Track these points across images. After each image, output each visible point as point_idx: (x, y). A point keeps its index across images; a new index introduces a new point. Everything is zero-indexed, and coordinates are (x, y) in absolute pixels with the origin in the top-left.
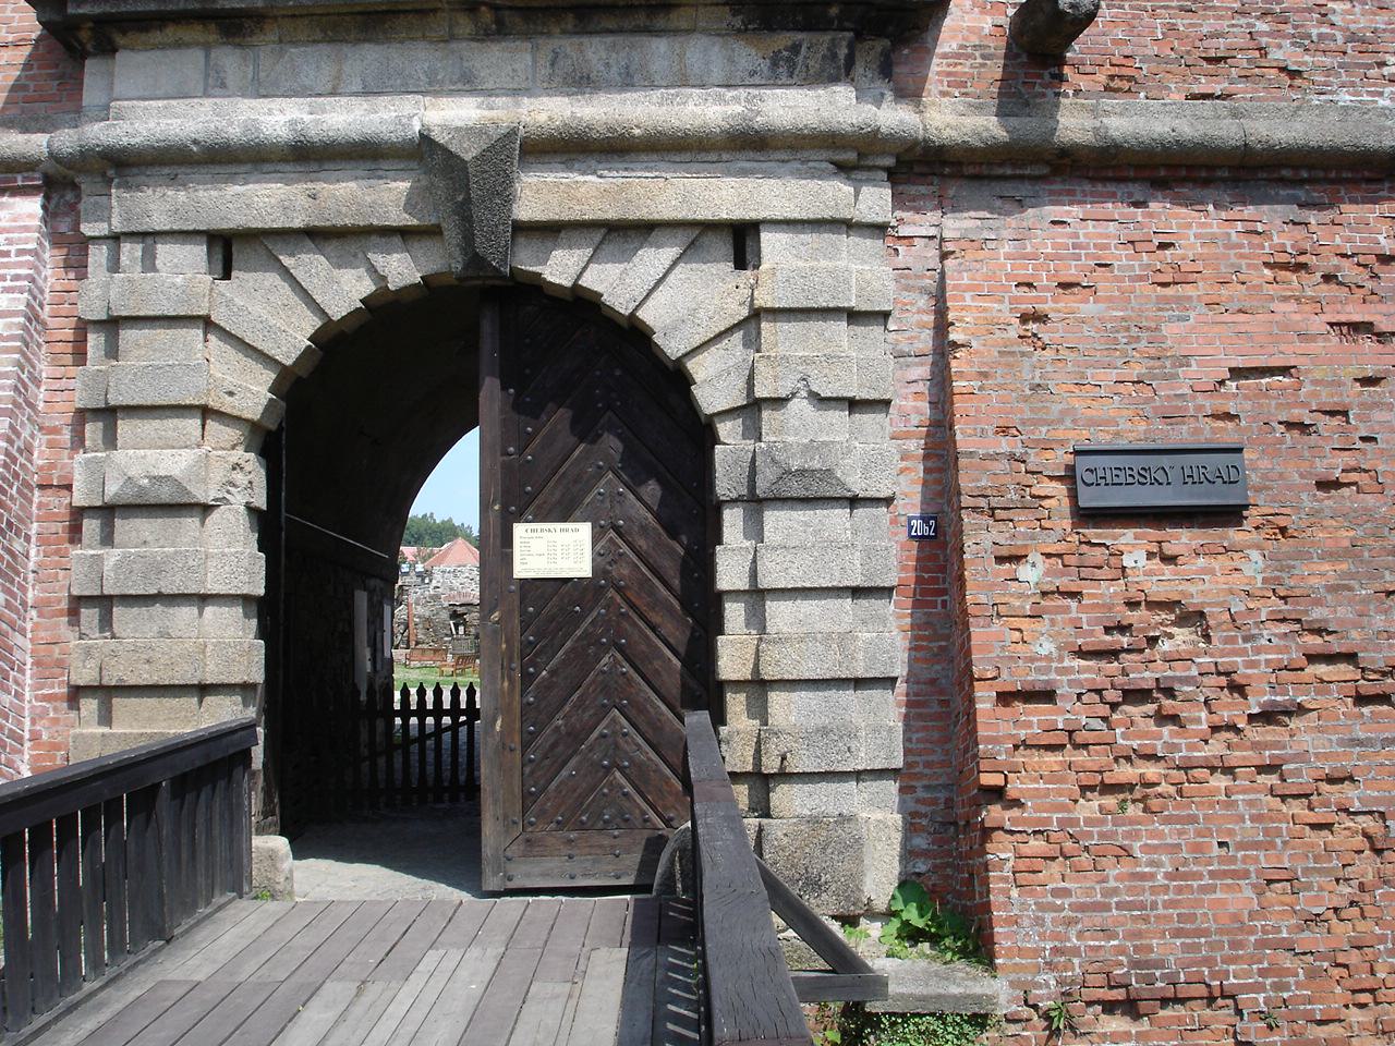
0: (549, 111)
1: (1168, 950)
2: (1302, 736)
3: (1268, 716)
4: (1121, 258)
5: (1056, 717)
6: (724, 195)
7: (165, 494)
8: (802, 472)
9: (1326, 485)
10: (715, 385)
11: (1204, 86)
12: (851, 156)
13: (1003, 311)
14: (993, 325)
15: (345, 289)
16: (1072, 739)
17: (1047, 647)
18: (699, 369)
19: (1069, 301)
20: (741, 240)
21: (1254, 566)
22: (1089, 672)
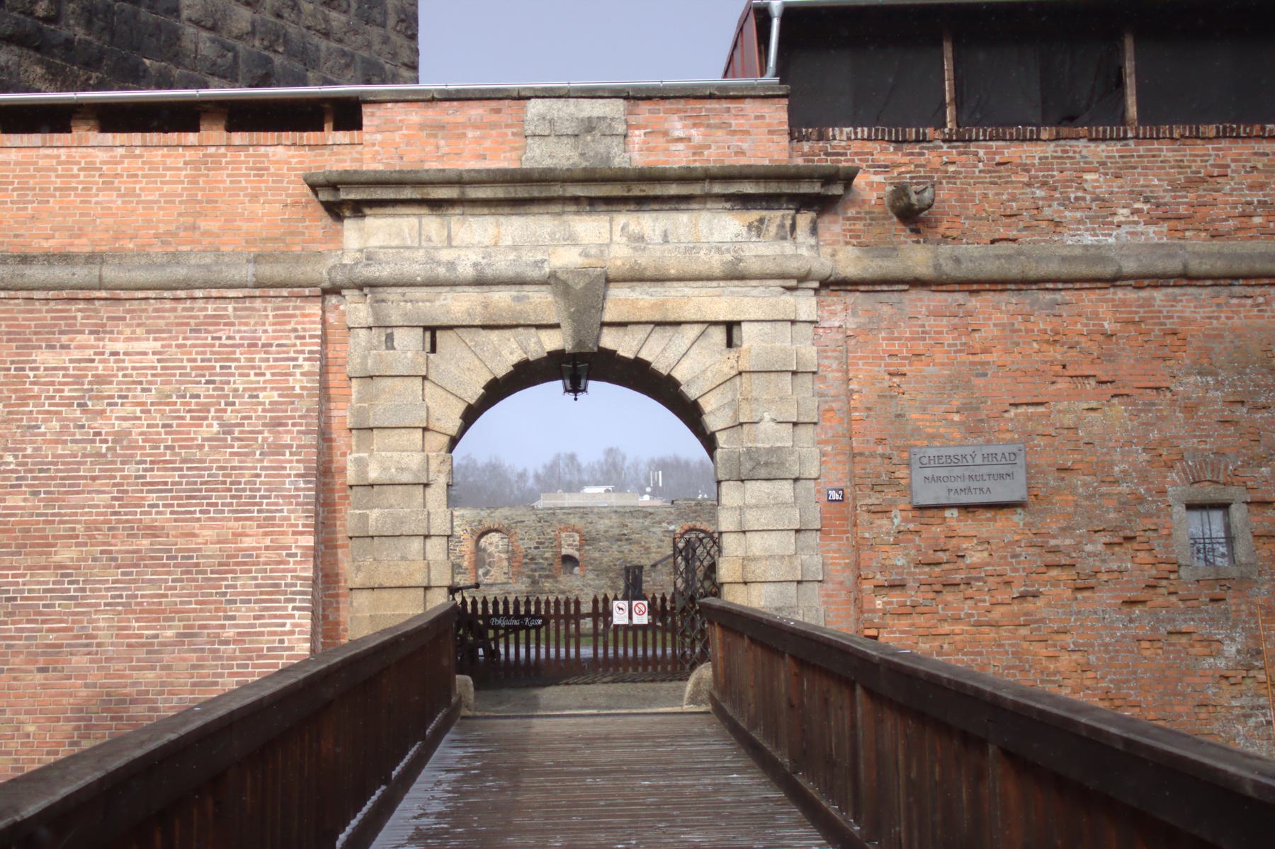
0: (620, 255)
3: (1023, 596)
4: (948, 339)
8: (766, 464)
11: (1002, 232)
12: (793, 283)
13: (880, 371)
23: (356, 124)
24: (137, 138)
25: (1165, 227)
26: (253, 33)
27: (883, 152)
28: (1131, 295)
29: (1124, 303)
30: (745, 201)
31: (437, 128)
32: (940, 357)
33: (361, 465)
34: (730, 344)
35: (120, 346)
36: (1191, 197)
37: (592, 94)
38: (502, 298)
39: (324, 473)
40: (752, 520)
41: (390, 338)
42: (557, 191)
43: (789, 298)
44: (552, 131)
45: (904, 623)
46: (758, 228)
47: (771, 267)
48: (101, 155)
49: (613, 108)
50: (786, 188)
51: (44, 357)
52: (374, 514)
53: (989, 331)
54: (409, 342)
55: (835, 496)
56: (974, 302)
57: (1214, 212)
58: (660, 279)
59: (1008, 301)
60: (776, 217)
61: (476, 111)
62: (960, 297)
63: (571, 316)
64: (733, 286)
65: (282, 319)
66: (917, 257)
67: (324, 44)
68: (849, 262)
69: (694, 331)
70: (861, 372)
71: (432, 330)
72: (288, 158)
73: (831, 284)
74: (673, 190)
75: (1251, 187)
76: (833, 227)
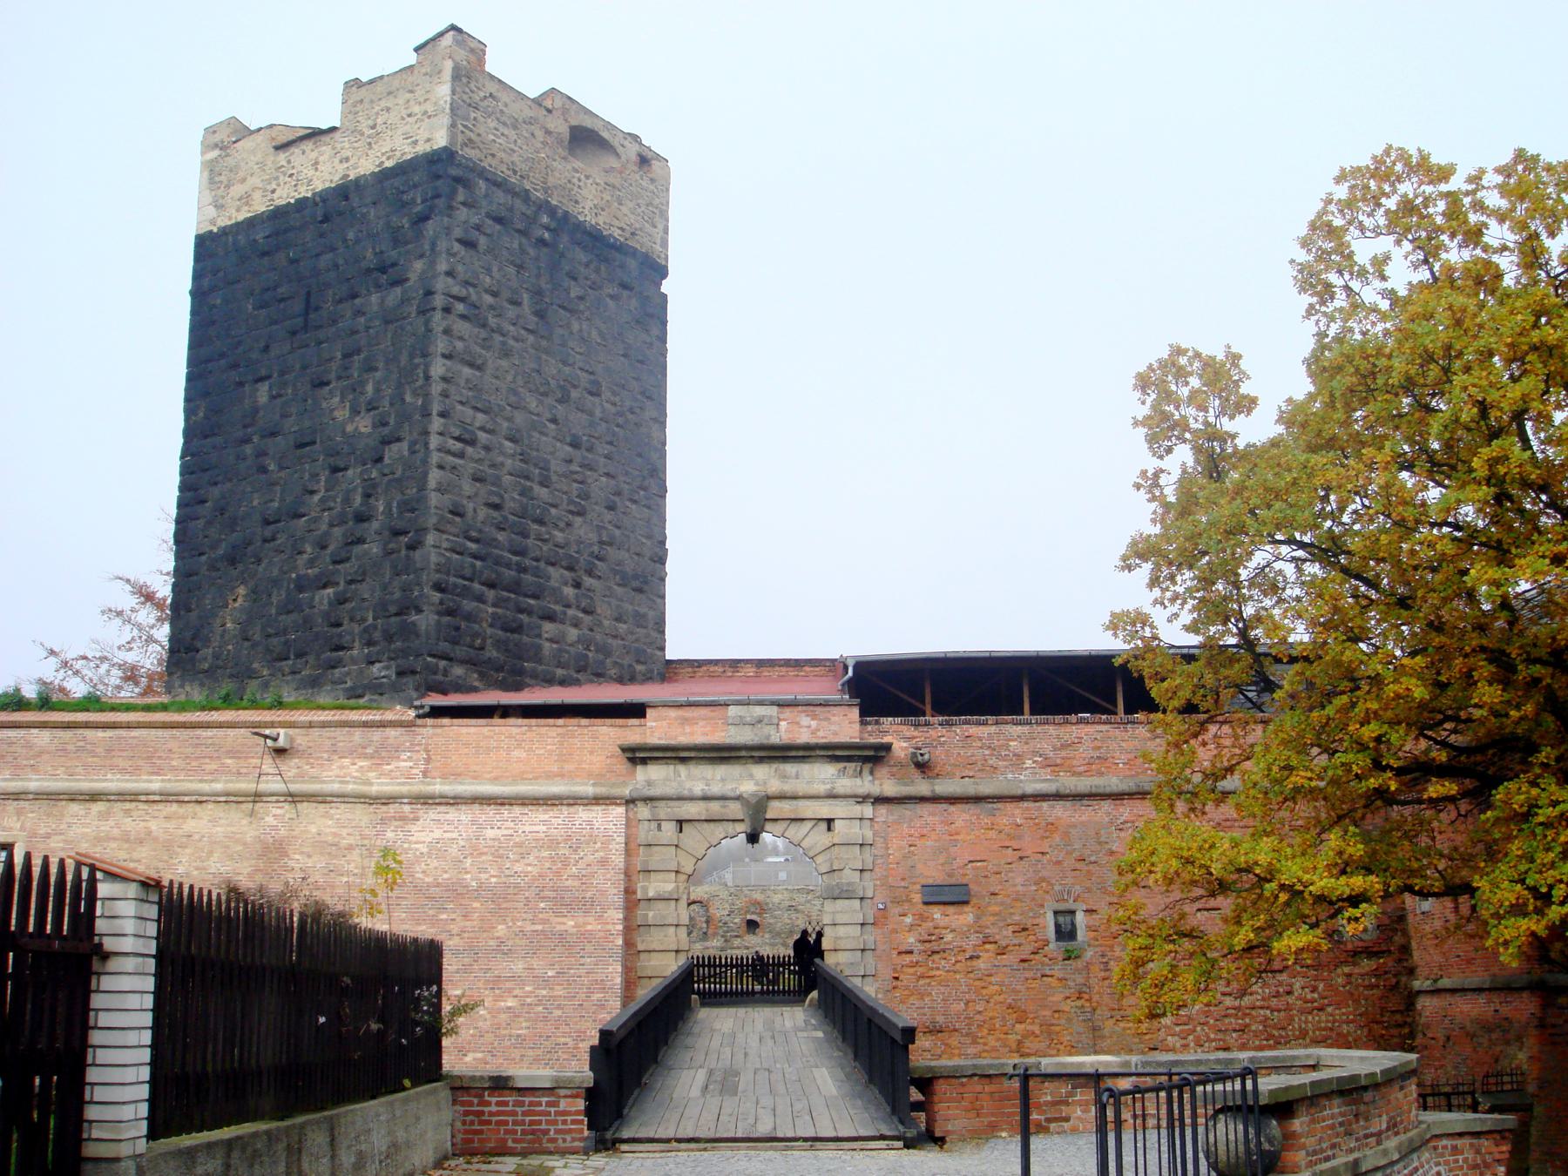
0: (775, 786)
1: (940, 1019)
3: (971, 958)
4: (939, 828)
5: (914, 958)
17: (912, 940)
20: (830, 821)
21: (970, 918)
23: (643, 715)
26: (579, 641)
27: (909, 731)
28: (1031, 805)
30: (837, 759)
31: (685, 721)
32: (934, 837)
33: (645, 889)
34: (829, 829)
35: (527, 828)
36: (1064, 753)
37: (761, 703)
38: (715, 807)
39: (629, 892)
40: (840, 919)
41: (659, 827)
43: (858, 807)
44: (741, 723)
45: (912, 970)
47: (849, 791)
49: (773, 711)
52: (651, 914)
53: (959, 823)
54: (669, 828)
56: (952, 808)
57: (1075, 762)
58: (795, 798)
59: (972, 809)
64: (830, 801)
66: (922, 787)
68: (890, 788)
69: (809, 825)
71: (680, 822)
72: (613, 734)
73: (880, 800)
74: (801, 753)
76: (883, 771)
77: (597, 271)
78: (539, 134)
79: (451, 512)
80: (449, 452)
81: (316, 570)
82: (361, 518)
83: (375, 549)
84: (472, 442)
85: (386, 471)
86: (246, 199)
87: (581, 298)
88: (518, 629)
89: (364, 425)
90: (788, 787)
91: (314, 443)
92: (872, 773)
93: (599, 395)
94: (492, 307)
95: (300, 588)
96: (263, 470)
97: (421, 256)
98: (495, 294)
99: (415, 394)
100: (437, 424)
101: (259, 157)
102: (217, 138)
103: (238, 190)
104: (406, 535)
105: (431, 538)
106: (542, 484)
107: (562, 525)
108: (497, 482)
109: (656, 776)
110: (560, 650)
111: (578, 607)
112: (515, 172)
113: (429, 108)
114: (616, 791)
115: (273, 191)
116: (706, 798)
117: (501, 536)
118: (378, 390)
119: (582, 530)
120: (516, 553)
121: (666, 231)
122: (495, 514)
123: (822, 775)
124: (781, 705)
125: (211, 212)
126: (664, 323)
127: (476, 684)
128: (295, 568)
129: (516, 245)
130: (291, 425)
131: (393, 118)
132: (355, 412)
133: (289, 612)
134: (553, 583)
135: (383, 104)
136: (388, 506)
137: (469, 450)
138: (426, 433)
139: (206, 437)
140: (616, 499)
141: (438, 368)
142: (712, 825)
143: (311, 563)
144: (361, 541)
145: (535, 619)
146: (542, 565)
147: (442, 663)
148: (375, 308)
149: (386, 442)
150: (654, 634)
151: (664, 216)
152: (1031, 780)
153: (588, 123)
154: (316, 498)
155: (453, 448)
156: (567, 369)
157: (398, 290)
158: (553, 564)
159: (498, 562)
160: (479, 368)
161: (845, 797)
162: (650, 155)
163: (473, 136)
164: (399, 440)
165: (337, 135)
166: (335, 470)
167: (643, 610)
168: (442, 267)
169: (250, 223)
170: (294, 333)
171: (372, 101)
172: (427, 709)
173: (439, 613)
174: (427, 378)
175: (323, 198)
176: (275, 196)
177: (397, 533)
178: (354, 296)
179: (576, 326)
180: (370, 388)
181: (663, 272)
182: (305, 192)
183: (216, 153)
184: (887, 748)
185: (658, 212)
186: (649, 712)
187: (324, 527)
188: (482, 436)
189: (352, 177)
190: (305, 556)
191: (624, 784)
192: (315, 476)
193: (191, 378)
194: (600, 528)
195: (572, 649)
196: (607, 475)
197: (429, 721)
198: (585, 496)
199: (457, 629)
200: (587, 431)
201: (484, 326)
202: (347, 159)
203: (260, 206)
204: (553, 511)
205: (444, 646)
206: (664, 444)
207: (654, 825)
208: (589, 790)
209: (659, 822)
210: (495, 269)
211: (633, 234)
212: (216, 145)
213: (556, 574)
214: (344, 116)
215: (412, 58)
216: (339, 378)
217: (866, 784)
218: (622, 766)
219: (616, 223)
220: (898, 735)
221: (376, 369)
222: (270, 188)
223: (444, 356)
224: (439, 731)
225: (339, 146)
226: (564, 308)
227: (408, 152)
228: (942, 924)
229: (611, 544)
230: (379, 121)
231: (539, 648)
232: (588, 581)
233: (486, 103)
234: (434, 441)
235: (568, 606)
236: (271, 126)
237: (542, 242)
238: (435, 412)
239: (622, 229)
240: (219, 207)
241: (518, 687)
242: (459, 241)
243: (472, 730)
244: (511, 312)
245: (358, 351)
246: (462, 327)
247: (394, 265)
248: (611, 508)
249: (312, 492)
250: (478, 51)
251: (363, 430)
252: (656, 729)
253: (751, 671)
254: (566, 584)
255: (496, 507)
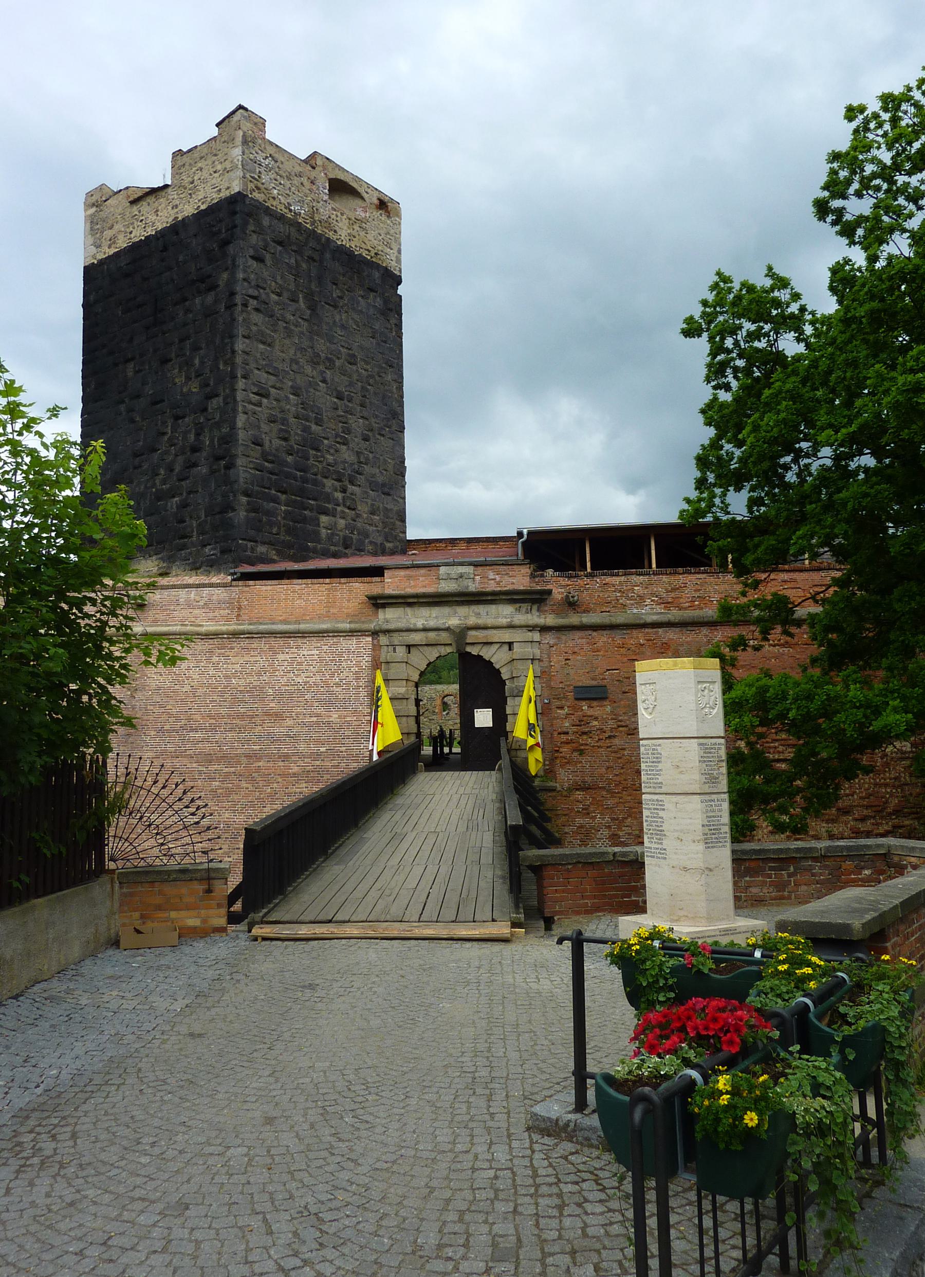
0: (472, 621)
2: (616, 741)
6: (507, 636)
7: (400, 696)
9: (624, 692)
10: (505, 675)
11: (605, 609)
14: (559, 661)
15: (433, 654)
16: (572, 741)
17: (567, 724)
18: (503, 671)
19: (574, 656)
20: (510, 644)
21: (608, 709)
22: (575, 729)
24: (309, 581)
25: (663, 606)
28: (650, 630)
29: (648, 633)
31: (409, 578)
34: (510, 650)
35: (305, 653)
36: (673, 595)
37: (462, 564)
38: (432, 635)
41: (394, 649)
42: (450, 599)
43: (530, 634)
44: (449, 578)
46: (518, 610)
47: (523, 623)
48: (298, 587)
49: (470, 569)
50: (526, 597)
51: (281, 657)
53: (600, 644)
54: (401, 652)
55: (546, 701)
58: (485, 628)
60: (525, 606)
61: (423, 571)
62: (590, 632)
63: (456, 642)
64: (511, 630)
65: (359, 643)
66: (574, 619)
67: (371, 528)
68: (550, 620)
70: (555, 659)
72: (360, 588)
75: (695, 591)
77: (351, 279)
78: (307, 184)
79: (253, 443)
80: (250, 403)
81: (168, 486)
82: (195, 449)
83: (203, 470)
84: (266, 396)
85: (209, 417)
86: (113, 241)
87: (341, 298)
88: (304, 520)
89: (194, 387)
90: (480, 622)
91: (164, 401)
92: (538, 610)
93: (355, 364)
94: (277, 303)
95: (159, 499)
96: (132, 421)
97: (227, 269)
98: (279, 295)
99: (226, 363)
100: (241, 384)
101: (120, 210)
102: (94, 198)
103: (108, 234)
104: (224, 457)
105: (240, 461)
106: (317, 424)
107: (332, 451)
108: (284, 421)
109: (391, 617)
110: (332, 534)
111: (344, 505)
112: (291, 211)
113: (228, 165)
114: (365, 626)
115: (131, 233)
116: (425, 630)
117: (290, 459)
118: (202, 363)
119: (346, 455)
120: (300, 471)
121: (399, 251)
122: (284, 443)
123: (504, 613)
124: (476, 565)
125: (93, 250)
126: (400, 315)
127: (275, 557)
128: (154, 485)
129: (293, 261)
130: (149, 390)
131: (205, 174)
132: (188, 378)
133: (152, 514)
134: (327, 490)
135: (200, 165)
136: (212, 441)
137: (265, 401)
138: (234, 390)
139: (96, 401)
140: (370, 434)
141: (240, 345)
142: (430, 648)
143: (164, 482)
144: (195, 465)
145: (314, 514)
146: (319, 477)
147: (250, 544)
148: (199, 307)
149: (209, 397)
150: (398, 523)
151: (398, 241)
152: (650, 612)
153: (341, 176)
154: (166, 438)
155: (253, 400)
156: (333, 347)
157: (213, 293)
158: (326, 477)
159: (288, 476)
160: (269, 345)
161: (521, 627)
162: (386, 199)
163: (260, 185)
164: (217, 396)
165: (170, 190)
166: (177, 418)
167: (388, 507)
168: (241, 276)
169: (116, 255)
170: (148, 328)
171: (190, 165)
172: (239, 575)
173: (246, 511)
174: (233, 352)
175: (161, 235)
176: (132, 235)
177: (218, 458)
178: (185, 300)
179: (337, 318)
180: (197, 361)
181: (398, 280)
182: (151, 231)
183: (94, 209)
184: (549, 592)
185: (393, 239)
186: (386, 573)
187: (171, 458)
188: (273, 391)
189: (180, 218)
190: (161, 477)
191: (371, 621)
192: (164, 423)
193: (84, 363)
194: (358, 454)
195: (341, 534)
196: (362, 417)
197: (240, 583)
198: (348, 431)
199: (260, 521)
200: (348, 389)
201: (272, 316)
202: (176, 206)
203: (122, 243)
204: (326, 442)
205: (252, 533)
206: (402, 397)
207: (391, 648)
208: (347, 626)
209: (394, 646)
210: (278, 277)
211: (376, 254)
212: (93, 205)
213: (329, 483)
214: (173, 176)
215: (215, 132)
216: (177, 356)
217: (535, 618)
218: (370, 611)
219: (363, 246)
220: (558, 585)
221: (201, 349)
222: (128, 230)
223: (244, 337)
224: (247, 589)
225: (170, 197)
226: (329, 304)
227: (215, 197)
228: (589, 713)
229: (366, 464)
230: (196, 178)
231: (317, 533)
232: (351, 488)
233: (267, 162)
234: (240, 396)
235: (338, 505)
236: (127, 188)
237: (311, 258)
238: (239, 376)
239: (369, 251)
240: (98, 246)
241: (304, 559)
242: (252, 257)
243: (269, 588)
244: (293, 307)
245: (188, 338)
246: (256, 318)
247: (210, 276)
248: (366, 439)
249: (164, 434)
250: (261, 123)
251: (194, 390)
252: (392, 584)
253: (463, 546)
254: (336, 491)
255: (285, 439)
